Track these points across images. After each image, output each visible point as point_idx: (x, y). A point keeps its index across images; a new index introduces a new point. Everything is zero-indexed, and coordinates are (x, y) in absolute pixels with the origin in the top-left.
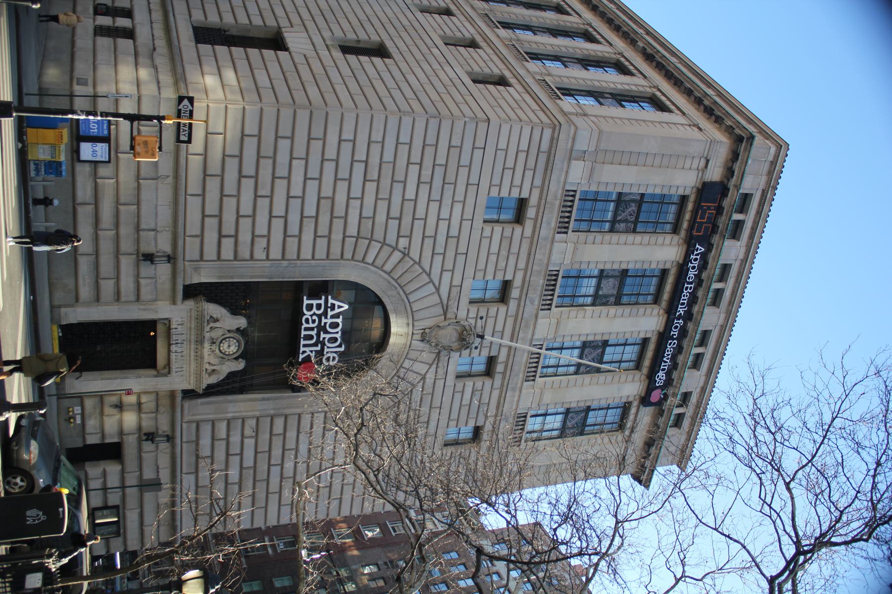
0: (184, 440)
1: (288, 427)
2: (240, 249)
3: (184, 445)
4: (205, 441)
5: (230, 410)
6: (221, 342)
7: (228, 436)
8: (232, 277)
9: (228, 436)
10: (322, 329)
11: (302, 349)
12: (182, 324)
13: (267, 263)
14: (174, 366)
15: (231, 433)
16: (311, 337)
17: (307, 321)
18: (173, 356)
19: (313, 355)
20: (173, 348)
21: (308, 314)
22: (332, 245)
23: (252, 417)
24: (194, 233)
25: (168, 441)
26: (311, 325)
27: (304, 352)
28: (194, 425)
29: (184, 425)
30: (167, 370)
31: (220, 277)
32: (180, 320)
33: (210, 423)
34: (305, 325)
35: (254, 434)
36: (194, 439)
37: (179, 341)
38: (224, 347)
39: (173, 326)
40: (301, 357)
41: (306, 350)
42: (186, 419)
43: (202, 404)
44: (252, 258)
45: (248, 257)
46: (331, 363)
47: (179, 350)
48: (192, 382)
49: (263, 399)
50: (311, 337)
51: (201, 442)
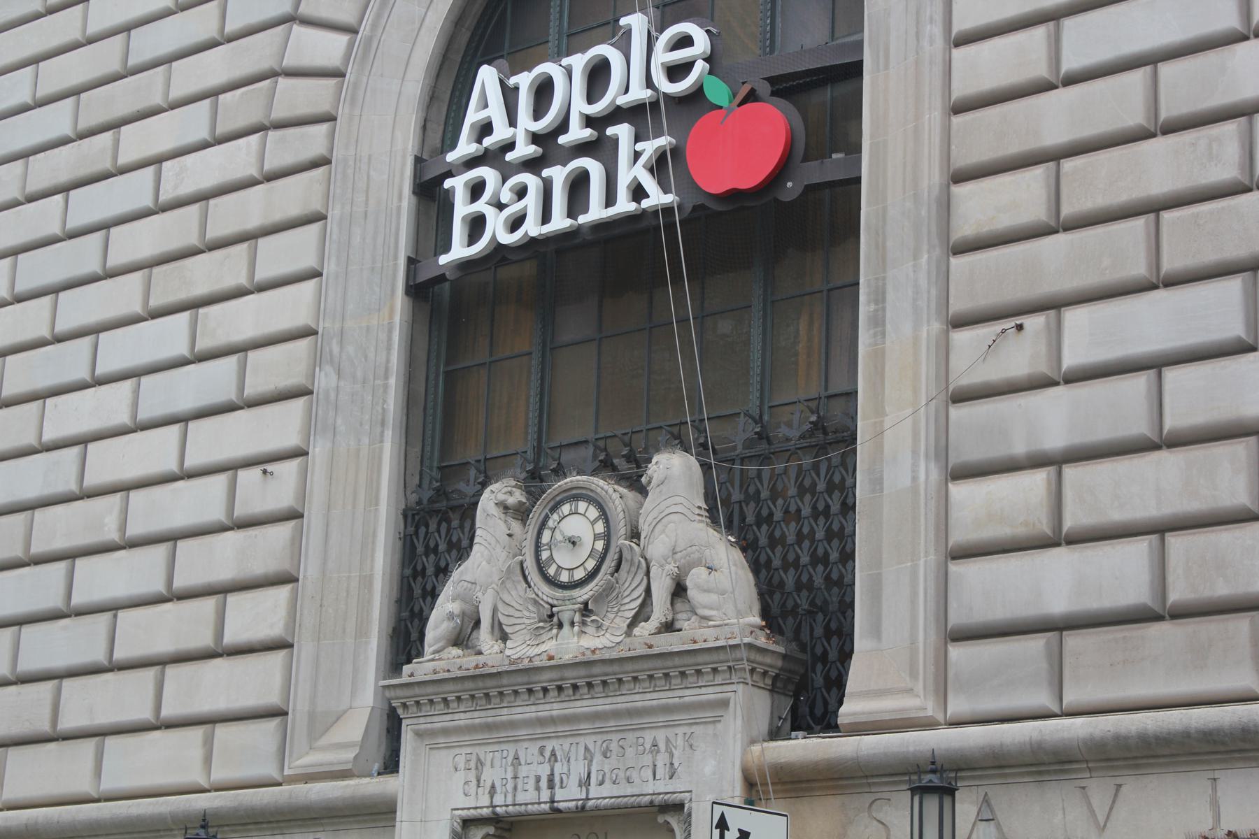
0: (1042, 699)
1: (1014, 147)
2: (258, 567)
3: (1072, 697)
4: (1057, 582)
5: (907, 482)
6: (552, 582)
7: (1036, 462)
8: (367, 581)
9: (1036, 462)
10: (548, 146)
11: (624, 205)
12: (480, 763)
13: (318, 450)
14: (650, 786)
15: (1019, 448)
16: (579, 184)
17: (516, 223)
18: (601, 794)
19: (649, 148)
20: (569, 796)
21: (497, 229)
22: (277, 216)
23: (945, 350)
24: (197, 753)
25: (948, 792)
26: (532, 202)
27: (638, 192)
28: (957, 652)
29: (958, 705)
30: (674, 822)
31: (361, 633)
32: (460, 777)
33: (955, 568)
34: (532, 228)
35: (1034, 323)
36: (1036, 645)
37: (544, 771)
38: (569, 562)
39: (479, 803)
40: (657, 198)
41: (633, 181)
42: (920, 703)
43: (876, 631)
44: (294, 515)
45: (282, 532)
46: (702, 43)
47: (579, 768)
48: (708, 694)
49: (878, 321)
50: (579, 184)
51: (1058, 604)
